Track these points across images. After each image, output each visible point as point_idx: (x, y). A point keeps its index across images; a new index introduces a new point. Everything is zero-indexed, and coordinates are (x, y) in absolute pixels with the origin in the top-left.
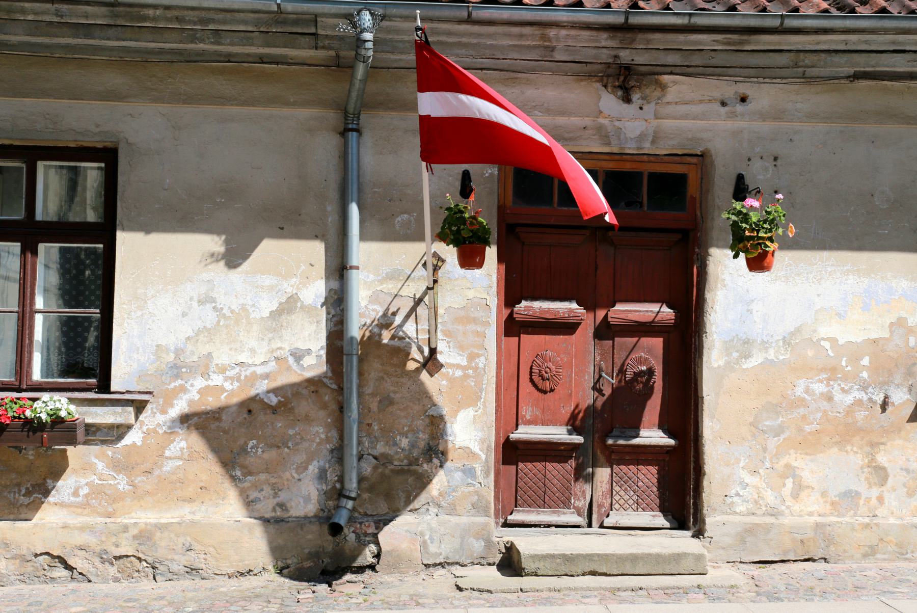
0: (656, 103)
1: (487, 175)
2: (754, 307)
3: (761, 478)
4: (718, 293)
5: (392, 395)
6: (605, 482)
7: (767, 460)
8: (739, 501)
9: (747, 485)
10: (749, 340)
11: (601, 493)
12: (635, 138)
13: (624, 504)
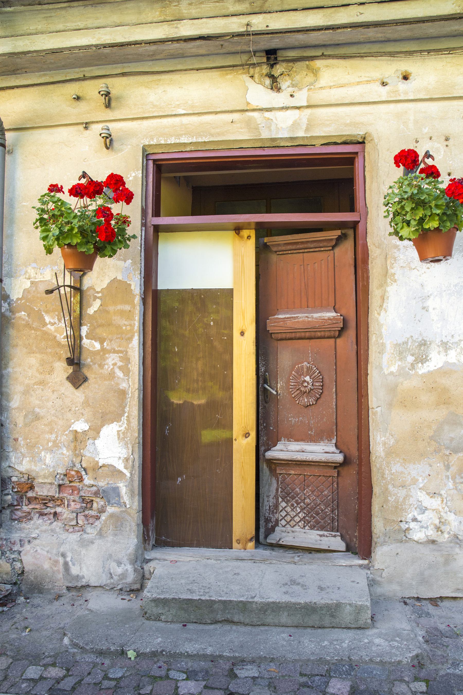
0: (308, 89)
1: (131, 178)
2: (430, 303)
3: (443, 501)
4: (388, 289)
5: (37, 410)
6: (272, 497)
7: (450, 480)
8: (416, 527)
9: (426, 509)
10: (425, 341)
11: (268, 508)
12: (287, 128)
13: (291, 520)
